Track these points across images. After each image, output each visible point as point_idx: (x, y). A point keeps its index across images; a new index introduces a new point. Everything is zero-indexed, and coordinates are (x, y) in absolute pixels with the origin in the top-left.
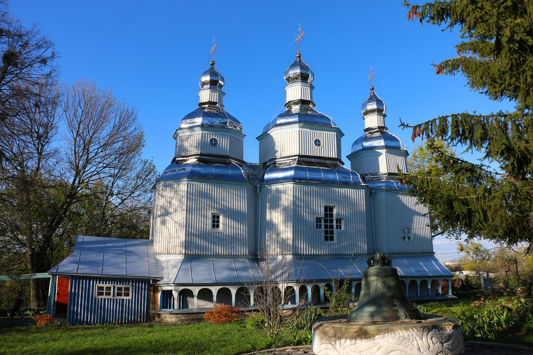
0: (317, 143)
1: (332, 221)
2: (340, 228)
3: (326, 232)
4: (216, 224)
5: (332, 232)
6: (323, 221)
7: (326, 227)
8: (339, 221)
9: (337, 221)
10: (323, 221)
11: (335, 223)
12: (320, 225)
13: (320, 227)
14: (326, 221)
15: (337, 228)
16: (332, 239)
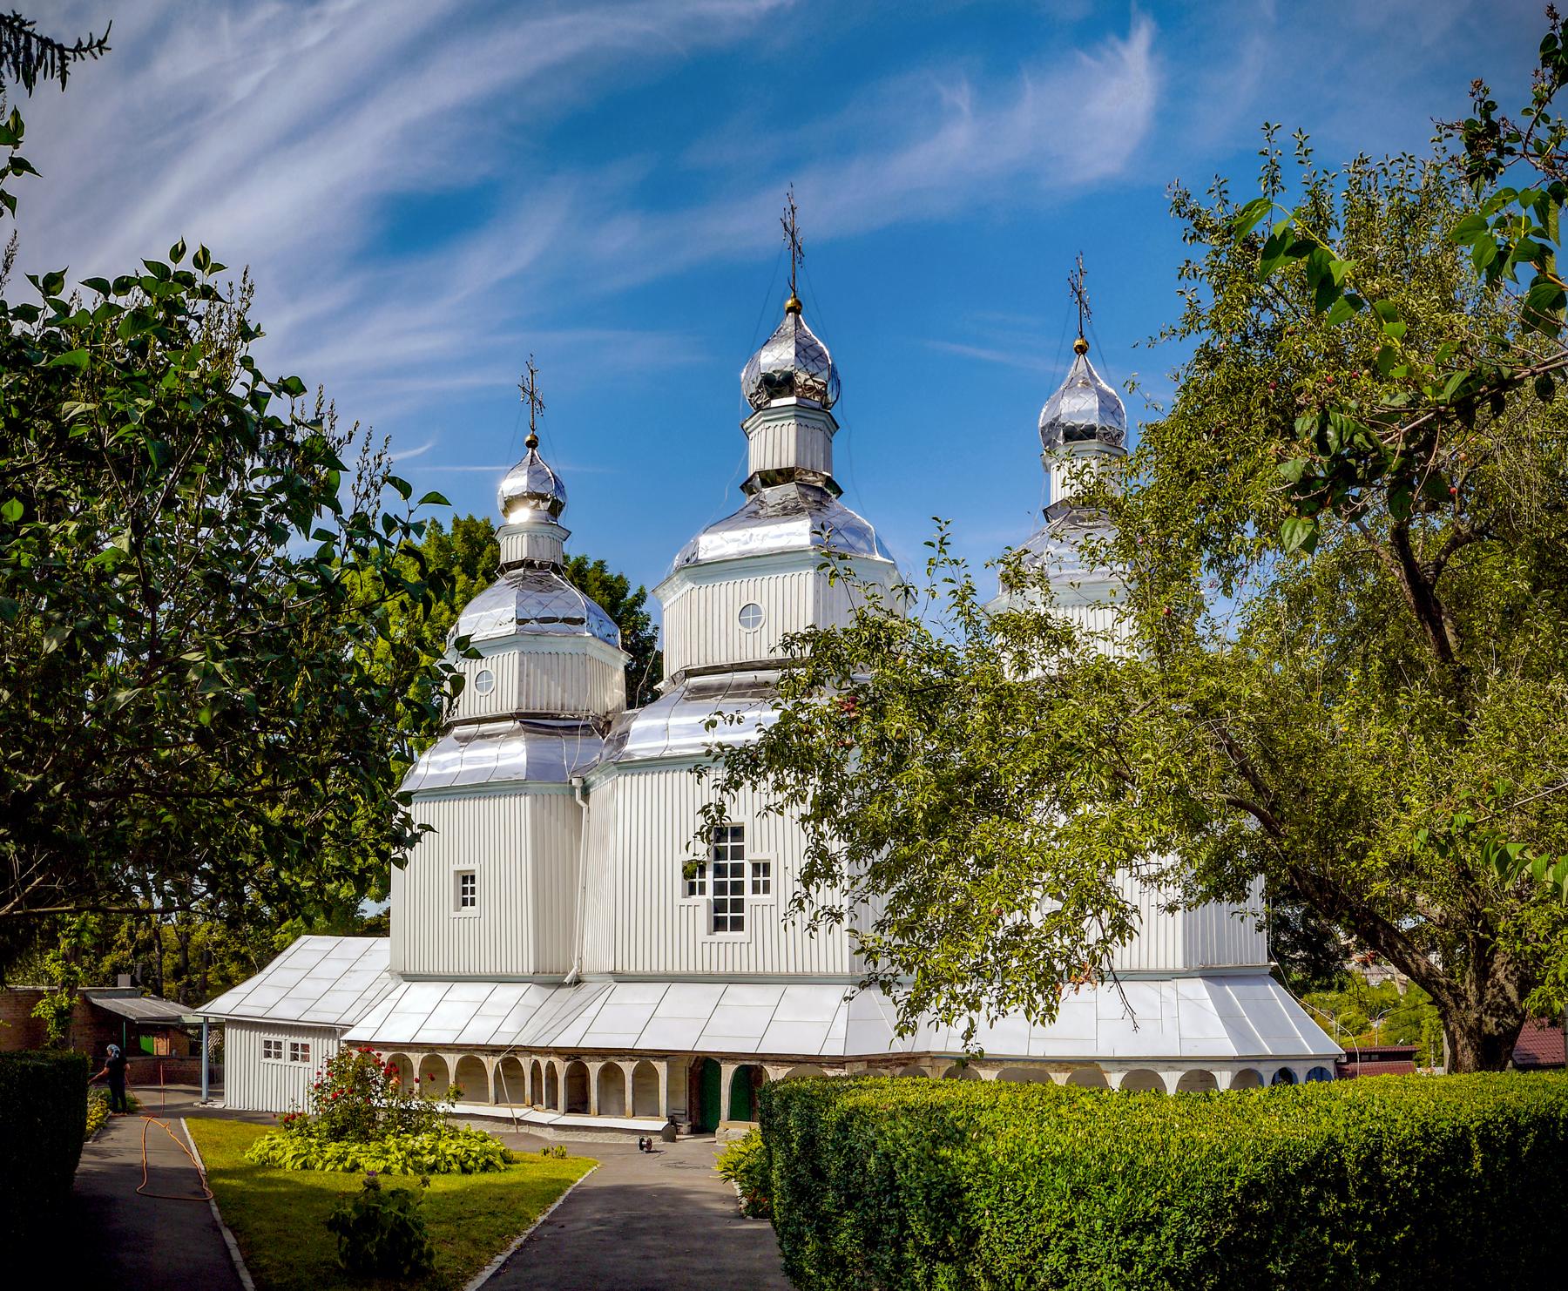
0: (749, 614)
1: (738, 870)
2: (767, 890)
3: (719, 906)
4: (469, 896)
5: (738, 906)
6: (709, 874)
7: (720, 888)
8: (762, 868)
9: (756, 866)
10: (709, 874)
11: (748, 879)
12: (702, 885)
13: (702, 892)
14: (719, 870)
15: (755, 890)
16: (738, 924)
